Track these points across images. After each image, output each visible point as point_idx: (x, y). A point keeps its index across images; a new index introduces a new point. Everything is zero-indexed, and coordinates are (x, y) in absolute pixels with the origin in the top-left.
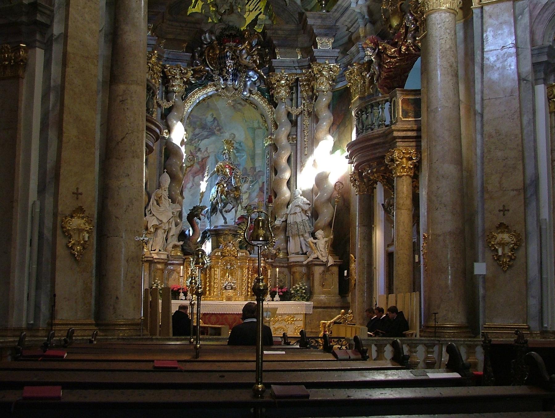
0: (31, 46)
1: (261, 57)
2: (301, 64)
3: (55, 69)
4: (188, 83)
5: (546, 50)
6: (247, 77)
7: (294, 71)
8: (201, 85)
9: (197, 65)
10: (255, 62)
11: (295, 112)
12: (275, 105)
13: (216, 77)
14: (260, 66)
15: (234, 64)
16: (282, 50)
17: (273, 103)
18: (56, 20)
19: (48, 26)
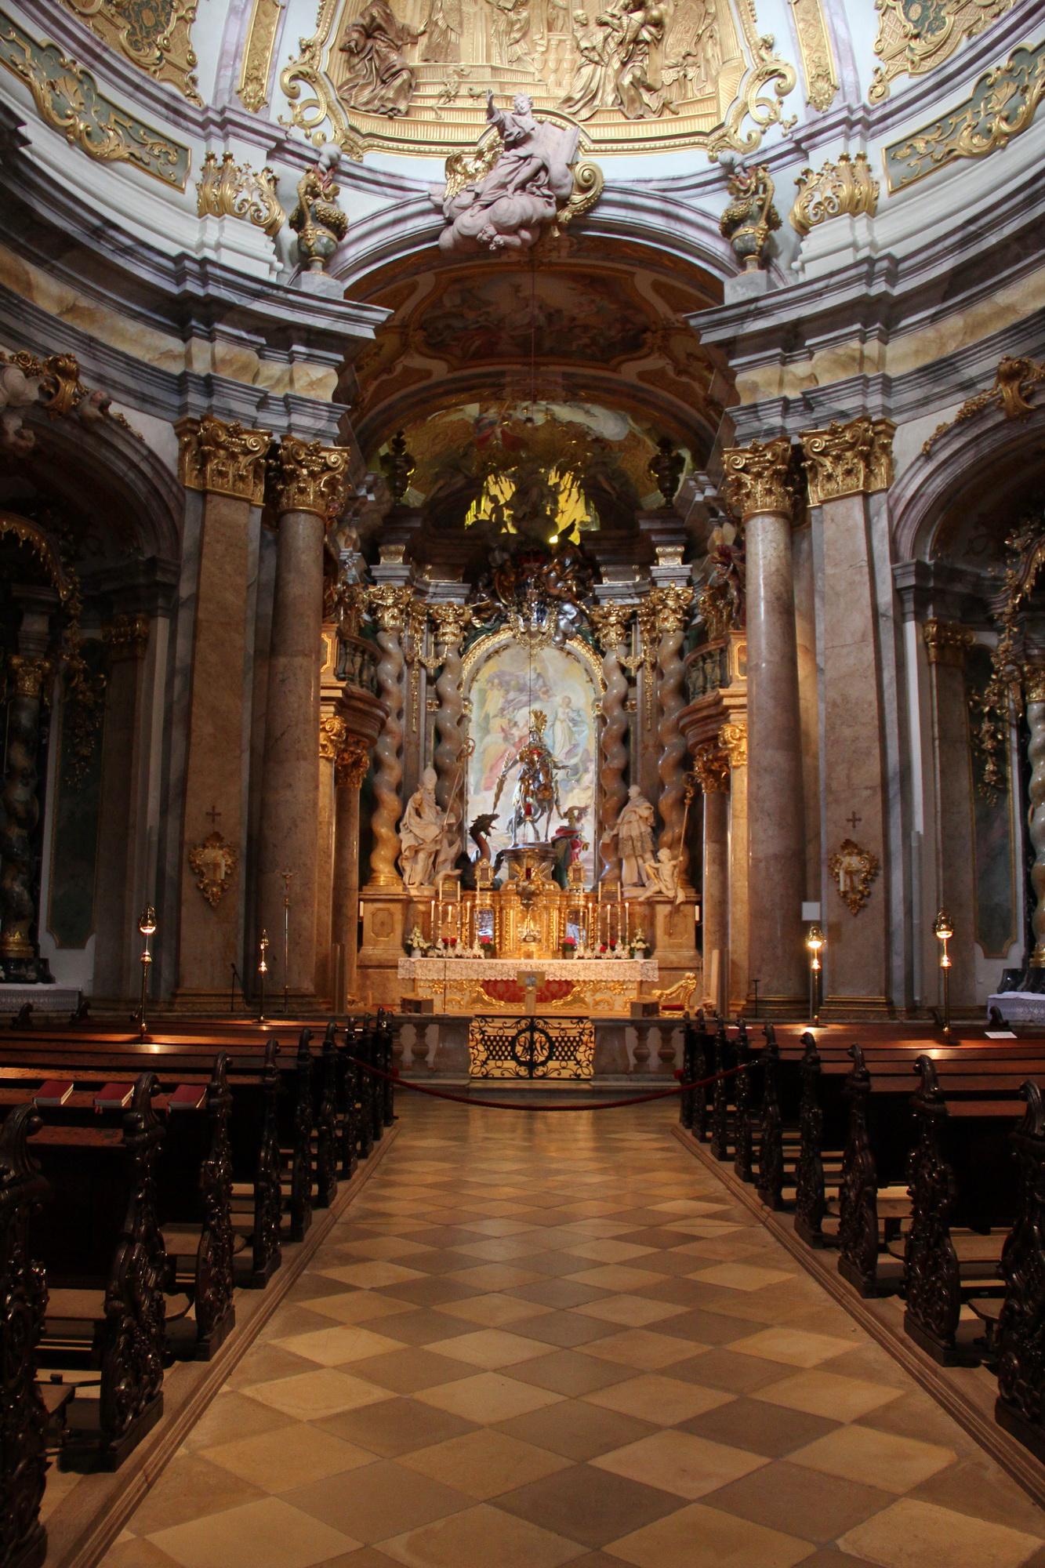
0: (151, 615)
1: (581, 582)
2: (639, 590)
3: (182, 645)
4: (468, 627)
5: (913, 568)
6: (559, 613)
7: (629, 601)
8: (489, 630)
9: (482, 600)
10: (570, 589)
11: (631, 663)
12: (603, 654)
13: (512, 617)
14: (579, 596)
15: (540, 594)
16: (610, 569)
17: (599, 650)
18: (184, 577)
19: (174, 587)
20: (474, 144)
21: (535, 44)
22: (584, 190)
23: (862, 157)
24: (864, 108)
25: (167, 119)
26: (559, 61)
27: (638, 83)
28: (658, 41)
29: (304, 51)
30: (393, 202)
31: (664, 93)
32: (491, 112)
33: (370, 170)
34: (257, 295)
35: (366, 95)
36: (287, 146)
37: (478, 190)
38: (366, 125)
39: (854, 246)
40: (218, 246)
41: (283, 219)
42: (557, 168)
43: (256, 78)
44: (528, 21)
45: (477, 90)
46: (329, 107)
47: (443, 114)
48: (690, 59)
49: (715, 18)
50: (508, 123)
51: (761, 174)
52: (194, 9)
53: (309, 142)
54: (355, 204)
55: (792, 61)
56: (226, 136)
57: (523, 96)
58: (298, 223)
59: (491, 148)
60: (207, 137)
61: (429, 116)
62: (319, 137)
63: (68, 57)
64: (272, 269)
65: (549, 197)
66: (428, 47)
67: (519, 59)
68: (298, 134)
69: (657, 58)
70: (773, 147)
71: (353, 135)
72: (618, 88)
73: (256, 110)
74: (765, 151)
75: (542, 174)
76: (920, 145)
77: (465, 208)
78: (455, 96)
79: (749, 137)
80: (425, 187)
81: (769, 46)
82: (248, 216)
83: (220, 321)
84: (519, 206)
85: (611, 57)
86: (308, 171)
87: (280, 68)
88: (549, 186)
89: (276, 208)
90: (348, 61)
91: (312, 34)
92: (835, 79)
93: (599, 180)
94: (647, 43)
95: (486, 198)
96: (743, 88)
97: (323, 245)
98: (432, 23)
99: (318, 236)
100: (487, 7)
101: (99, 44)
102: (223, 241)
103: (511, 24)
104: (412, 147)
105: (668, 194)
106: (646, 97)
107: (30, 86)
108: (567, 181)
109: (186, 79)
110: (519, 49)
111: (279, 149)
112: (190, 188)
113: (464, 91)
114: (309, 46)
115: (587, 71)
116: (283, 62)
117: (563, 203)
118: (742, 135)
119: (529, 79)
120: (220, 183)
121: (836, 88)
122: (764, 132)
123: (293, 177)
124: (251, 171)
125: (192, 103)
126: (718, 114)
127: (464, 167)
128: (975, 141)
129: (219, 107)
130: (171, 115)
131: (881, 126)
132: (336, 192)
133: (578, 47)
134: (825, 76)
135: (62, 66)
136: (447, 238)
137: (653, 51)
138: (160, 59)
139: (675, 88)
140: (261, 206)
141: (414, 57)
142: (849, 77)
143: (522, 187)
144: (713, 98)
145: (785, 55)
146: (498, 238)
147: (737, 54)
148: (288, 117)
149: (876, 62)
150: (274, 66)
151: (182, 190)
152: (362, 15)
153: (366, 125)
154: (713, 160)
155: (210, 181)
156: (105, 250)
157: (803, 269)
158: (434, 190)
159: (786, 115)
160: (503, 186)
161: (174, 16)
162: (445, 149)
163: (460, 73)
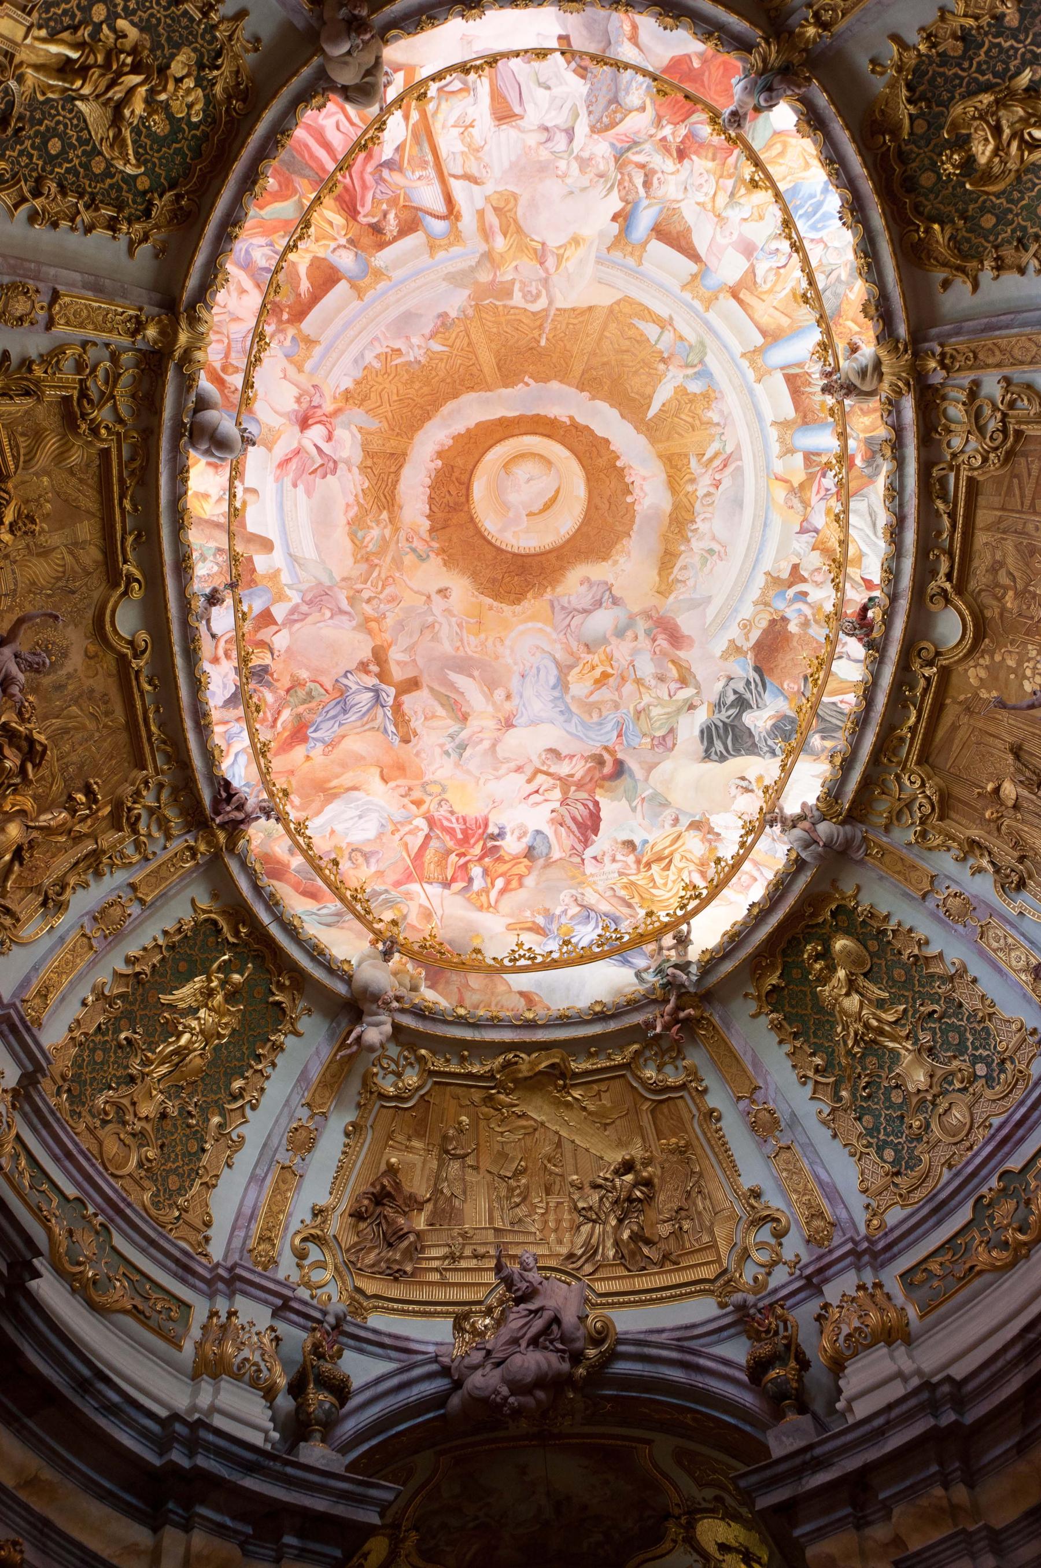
20: (479, 1303)
21: (534, 1207)
22: (597, 1342)
23: (878, 1285)
24: (867, 1238)
25: (175, 1275)
26: (559, 1221)
27: (634, 1237)
28: (649, 1199)
29: (315, 1215)
30: (392, 1366)
31: (663, 1246)
32: (499, 1268)
33: (375, 1331)
34: (250, 1468)
35: (372, 1257)
36: (295, 1305)
37: (489, 1346)
38: (371, 1287)
39: (900, 1375)
40: (213, 1409)
41: (282, 1382)
42: (569, 1318)
43: (270, 1239)
44: (527, 1187)
45: (481, 1250)
46: (336, 1268)
47: (448, 1274)
48: (683, 1213)
49: (701, 1175)
50: (516, 1277)
51: (779, 1311)
52: (217, 1176)
53: (315, 1302)
54: (360, 1368)
55: (782, 1206)
56: (231, 1296)
57: (529, 1252)
58: (297, 1388)
59: (501, 1302)
60: (211, 1296)
61: (435, 1277)
62: (325, 1297)
63: (91, 1210)
64: (266, 1440)
65: (563, 1351)
66: (434, 1213)
67: (520, 1220)
68: (304, 1293)
69: (652, 1215)
70: (783, 1286)
71: (357, 1296)
72: (617, 1244)
73: (265, 1269)
74: (775, 1291)
75: (555, 1327)
76: (934, 1266)
77: (474, 1368)
78: (461, 1257)
79: (756, 1279)
80: (431, 1349)
81: (756, 1194)
82: (247, 1377)
83: (203, 1502)
84: (531, 1361)
85: (607, 1215)
86: (314, 1329)
87: (292, 1230)
88: (563, 1340)
89: (278, 1369)
90: (355, 1226)
91: (324, 1200)
92: (829, 1215)
93: (612, 1332)
94: (639, 1200)
95: (498, 1355)
96: (740, 1235)
97: (325, 1412)
98: (437, 1191)
99: (319, 1399)
100: (489, 1177)
101: (124, 1200)
102: (217, 1403)
103: (511, 1190)
104: (417, 1308)
105: (685, 1342)
106: (646, 1251)
107: (49, 1231)
108: (580, 1333)
109: (200, 1237)
110: (521, 1212)
111: (284, 1307)
112: (188, 1346)
113: (468, 1252)
114: (321, 1211)
115: (586, 1229)
116: (295, 1225)
117: (577, 1357)
118: (747, 1278)
119: (531, 1239)
120: (220, 1342)
121: (833, 1225)
122: (769, 1274)
123: (297, 1337)
124: (254, 1330)
125: (204, 1260)
126: (719, 1260)
127: (473, 1325)
128: (994, 1254)
129: (229, 1264)
130: (180, 1271)
131: (888, 1255)
132: (339, 1354)
133: (576, 1208)
134: (821, 1215)
135: (84, 1217)
136: (455, 1401)
137: (646, 1208)
138: (178, 1218)
139: (672, 1240)
140: (262, 1365)
141: (421, 1222)
142: (843, 1215)
143: (534, 1342)
144: (713, 1246)
145: (774, 1201)
146: (511, 1400)
147: (728, 1204)
148: (295, 1277)
149: (864, 1199)
150: (286, 1228)
151: (180, 1348)
152: (373, 1185)
153: (371, 1287)
154: (722, 1305)
155: (212, 1338)
156: (87, 1408)
157: (850, 1409)
158: (443, 1349)
159: (788, 1255)
160: (515, 1341)
161: (198, 1182)
162: (451, 1309)
163: (464, 1235)
